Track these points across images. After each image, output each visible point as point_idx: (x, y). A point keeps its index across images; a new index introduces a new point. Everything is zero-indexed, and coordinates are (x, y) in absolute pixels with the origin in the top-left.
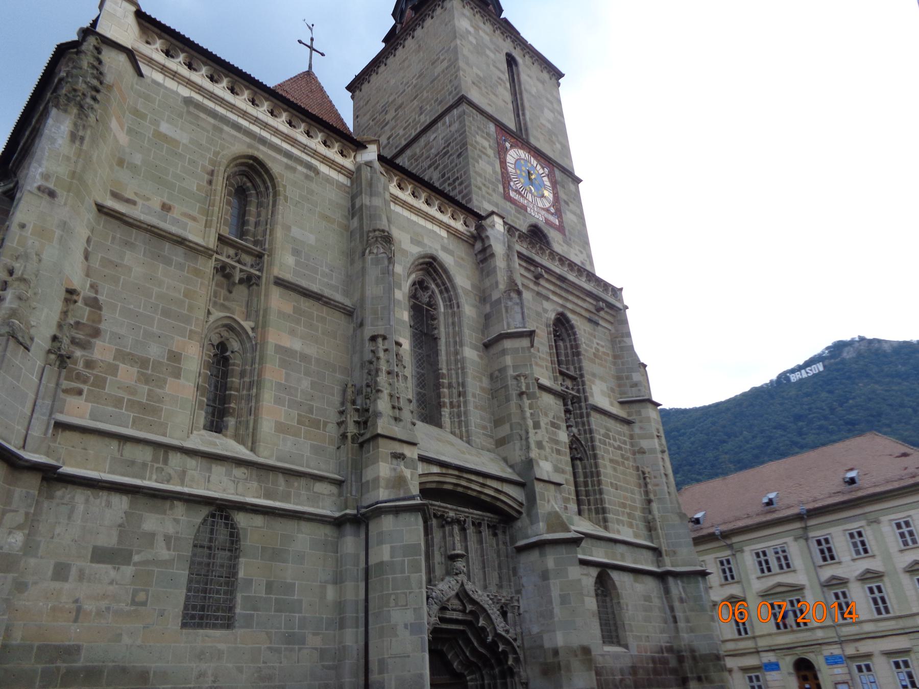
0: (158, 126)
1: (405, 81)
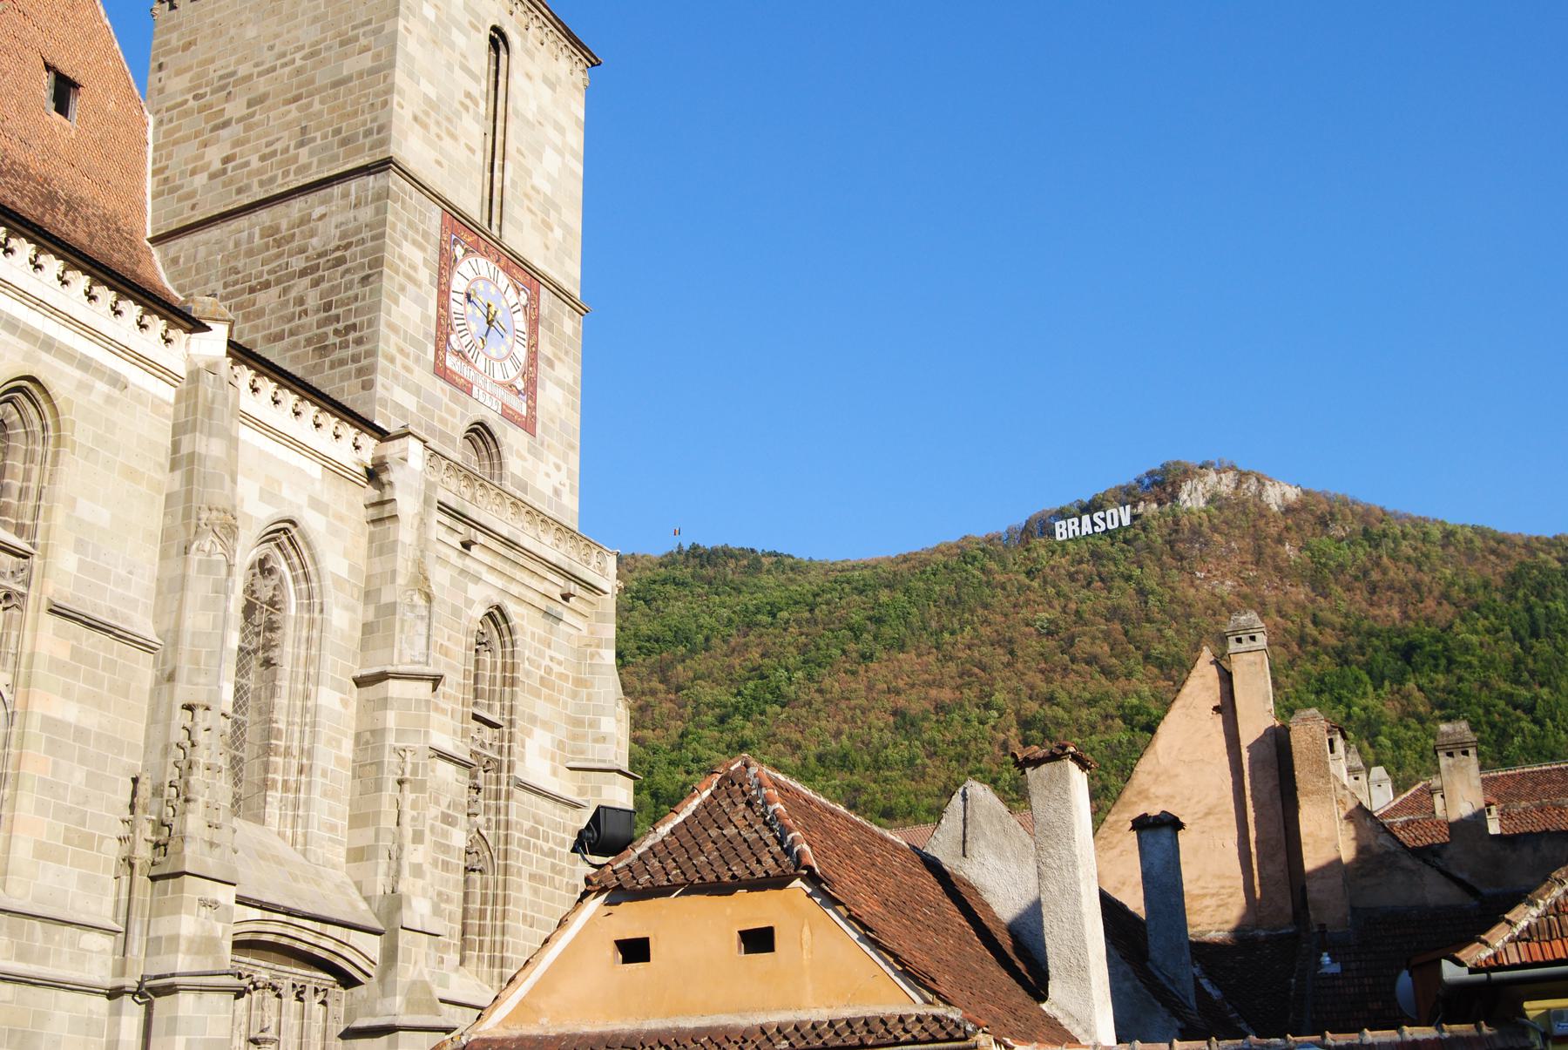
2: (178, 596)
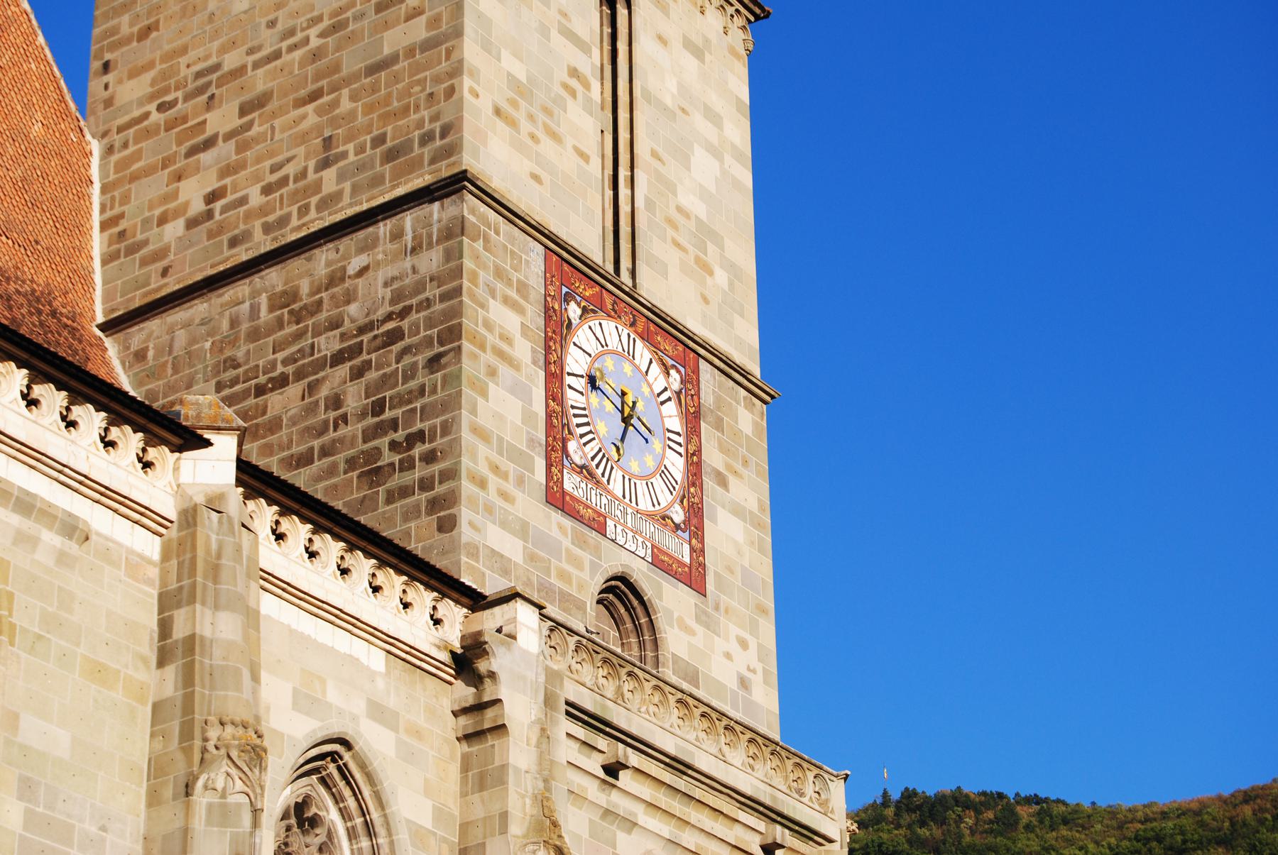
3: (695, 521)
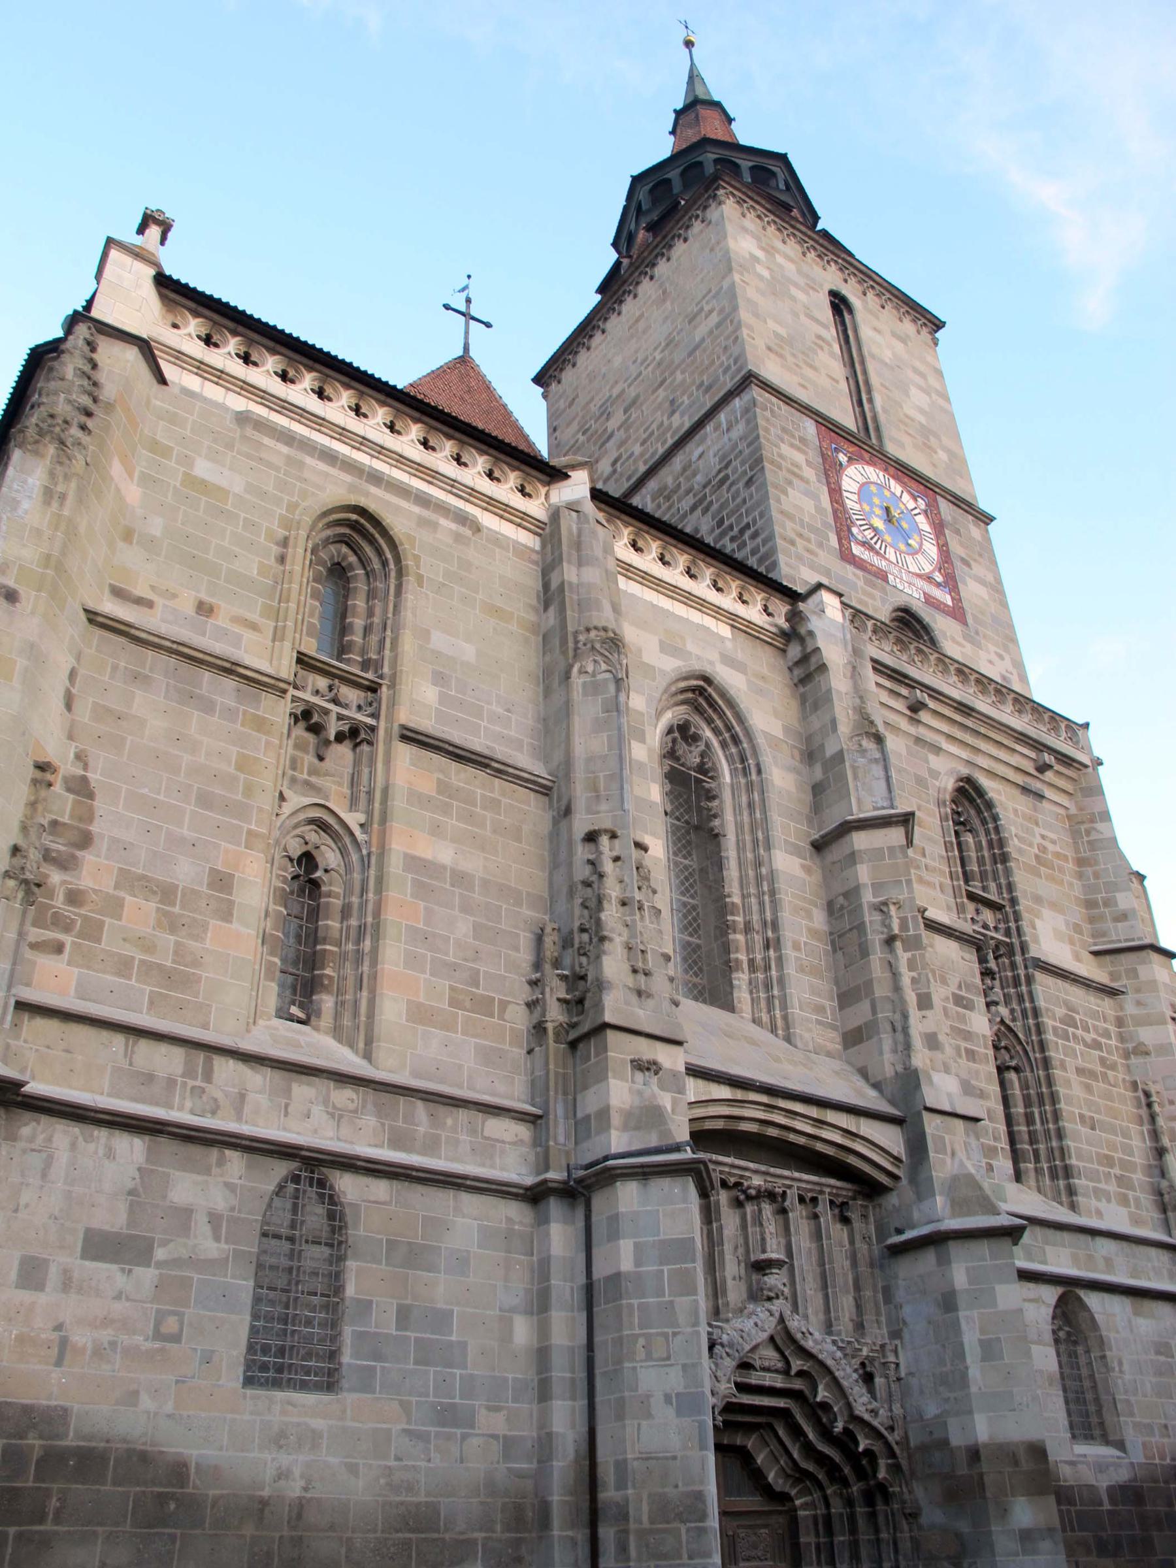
0: (191, 465)
1: (640, 356)
2: (564, 726)
3: (951, 583)
